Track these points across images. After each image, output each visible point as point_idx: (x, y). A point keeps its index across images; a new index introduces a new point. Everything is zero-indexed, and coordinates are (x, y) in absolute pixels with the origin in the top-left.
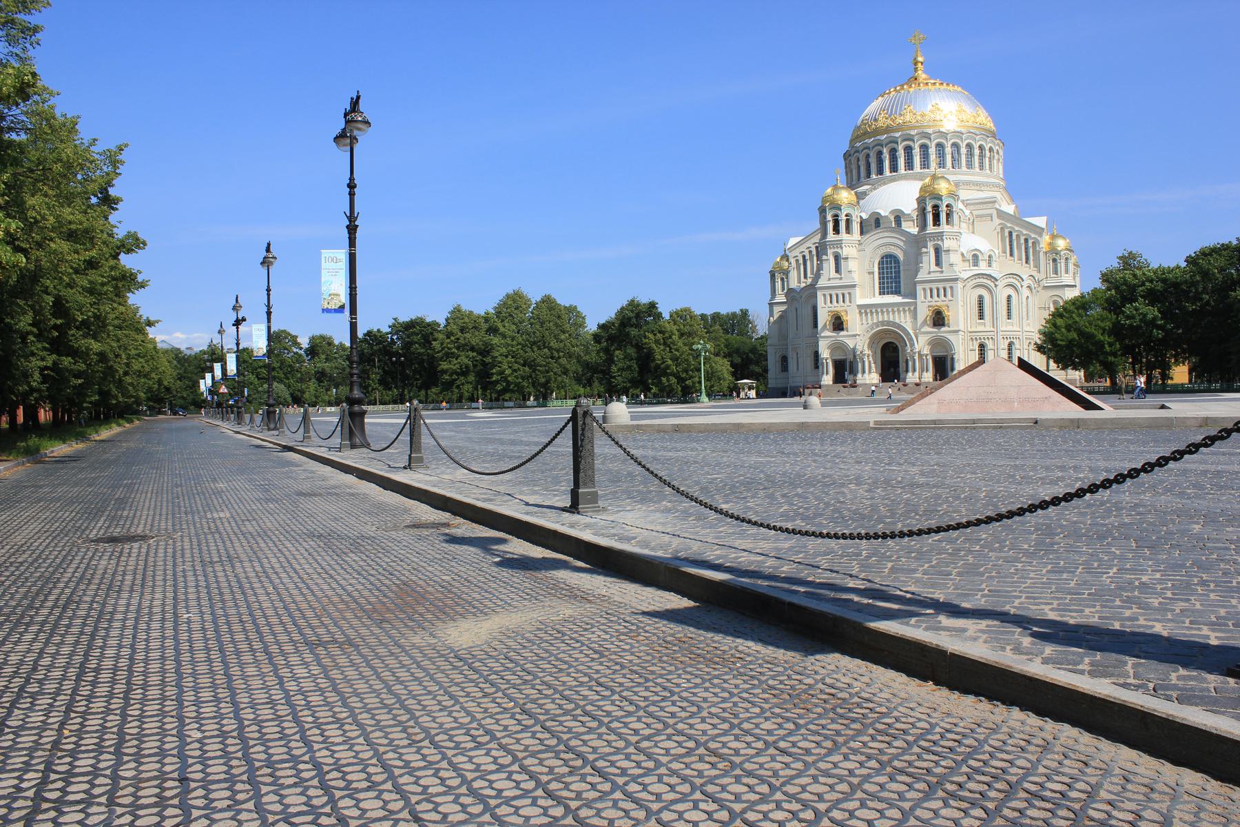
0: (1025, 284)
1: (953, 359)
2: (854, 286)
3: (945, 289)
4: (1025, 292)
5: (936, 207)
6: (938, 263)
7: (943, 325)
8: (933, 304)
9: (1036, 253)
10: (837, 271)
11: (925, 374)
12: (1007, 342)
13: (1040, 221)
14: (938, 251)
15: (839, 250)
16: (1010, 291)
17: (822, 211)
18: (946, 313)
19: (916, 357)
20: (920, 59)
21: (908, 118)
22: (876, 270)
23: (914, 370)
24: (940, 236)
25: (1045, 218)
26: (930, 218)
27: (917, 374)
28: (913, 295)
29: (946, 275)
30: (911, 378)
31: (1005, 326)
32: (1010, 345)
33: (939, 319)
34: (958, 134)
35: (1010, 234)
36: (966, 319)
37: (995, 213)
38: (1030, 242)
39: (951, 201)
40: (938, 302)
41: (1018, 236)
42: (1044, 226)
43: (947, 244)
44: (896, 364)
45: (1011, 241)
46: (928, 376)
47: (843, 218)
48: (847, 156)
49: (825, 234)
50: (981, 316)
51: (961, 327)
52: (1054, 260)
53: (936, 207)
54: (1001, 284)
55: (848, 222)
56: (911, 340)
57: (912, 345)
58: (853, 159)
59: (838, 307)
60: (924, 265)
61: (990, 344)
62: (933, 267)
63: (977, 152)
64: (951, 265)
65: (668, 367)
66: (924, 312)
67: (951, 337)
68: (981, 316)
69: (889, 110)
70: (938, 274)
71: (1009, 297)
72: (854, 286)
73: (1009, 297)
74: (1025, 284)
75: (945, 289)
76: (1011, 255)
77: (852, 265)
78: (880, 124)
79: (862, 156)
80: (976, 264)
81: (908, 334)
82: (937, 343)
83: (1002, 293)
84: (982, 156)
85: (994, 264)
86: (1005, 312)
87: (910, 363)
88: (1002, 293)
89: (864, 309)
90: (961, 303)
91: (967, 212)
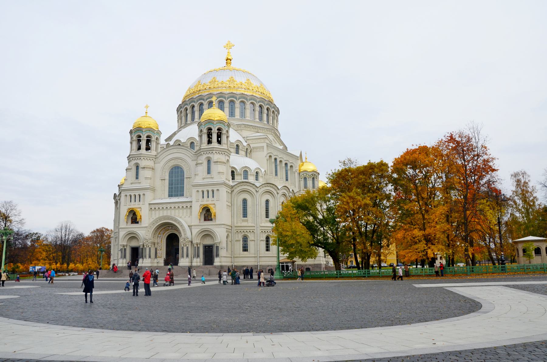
1: (217, 247)
3: (213, 191)
5: (210, 129)
7: (211, 220)
11: (195, 260)
15: (138, 161)
17: (131, 132)
18: (213, 211)
22: (167, 177)
30: (184, 262)
32: (268, 238)
33: (207, 214)
37: (265, 145)
38: (289, 165)
43: (215, 157)
46: (198, 262)
48: (178, 111)
50: (245, 215)
52: (305, 179)
55: (148, 141)
59: (134, 205)
61: (251, 237)
66: (197, 209)
71: (267, 202)
73: (267, 202)
74: (281, 192)
75: (213, 191)
76: (276, 175)
79: (183, 110)
80: (246, 177)
81: (182, 226)
84: (261, 112)
85: (260, 179)
89: (153, 207)
91: (245, 144)
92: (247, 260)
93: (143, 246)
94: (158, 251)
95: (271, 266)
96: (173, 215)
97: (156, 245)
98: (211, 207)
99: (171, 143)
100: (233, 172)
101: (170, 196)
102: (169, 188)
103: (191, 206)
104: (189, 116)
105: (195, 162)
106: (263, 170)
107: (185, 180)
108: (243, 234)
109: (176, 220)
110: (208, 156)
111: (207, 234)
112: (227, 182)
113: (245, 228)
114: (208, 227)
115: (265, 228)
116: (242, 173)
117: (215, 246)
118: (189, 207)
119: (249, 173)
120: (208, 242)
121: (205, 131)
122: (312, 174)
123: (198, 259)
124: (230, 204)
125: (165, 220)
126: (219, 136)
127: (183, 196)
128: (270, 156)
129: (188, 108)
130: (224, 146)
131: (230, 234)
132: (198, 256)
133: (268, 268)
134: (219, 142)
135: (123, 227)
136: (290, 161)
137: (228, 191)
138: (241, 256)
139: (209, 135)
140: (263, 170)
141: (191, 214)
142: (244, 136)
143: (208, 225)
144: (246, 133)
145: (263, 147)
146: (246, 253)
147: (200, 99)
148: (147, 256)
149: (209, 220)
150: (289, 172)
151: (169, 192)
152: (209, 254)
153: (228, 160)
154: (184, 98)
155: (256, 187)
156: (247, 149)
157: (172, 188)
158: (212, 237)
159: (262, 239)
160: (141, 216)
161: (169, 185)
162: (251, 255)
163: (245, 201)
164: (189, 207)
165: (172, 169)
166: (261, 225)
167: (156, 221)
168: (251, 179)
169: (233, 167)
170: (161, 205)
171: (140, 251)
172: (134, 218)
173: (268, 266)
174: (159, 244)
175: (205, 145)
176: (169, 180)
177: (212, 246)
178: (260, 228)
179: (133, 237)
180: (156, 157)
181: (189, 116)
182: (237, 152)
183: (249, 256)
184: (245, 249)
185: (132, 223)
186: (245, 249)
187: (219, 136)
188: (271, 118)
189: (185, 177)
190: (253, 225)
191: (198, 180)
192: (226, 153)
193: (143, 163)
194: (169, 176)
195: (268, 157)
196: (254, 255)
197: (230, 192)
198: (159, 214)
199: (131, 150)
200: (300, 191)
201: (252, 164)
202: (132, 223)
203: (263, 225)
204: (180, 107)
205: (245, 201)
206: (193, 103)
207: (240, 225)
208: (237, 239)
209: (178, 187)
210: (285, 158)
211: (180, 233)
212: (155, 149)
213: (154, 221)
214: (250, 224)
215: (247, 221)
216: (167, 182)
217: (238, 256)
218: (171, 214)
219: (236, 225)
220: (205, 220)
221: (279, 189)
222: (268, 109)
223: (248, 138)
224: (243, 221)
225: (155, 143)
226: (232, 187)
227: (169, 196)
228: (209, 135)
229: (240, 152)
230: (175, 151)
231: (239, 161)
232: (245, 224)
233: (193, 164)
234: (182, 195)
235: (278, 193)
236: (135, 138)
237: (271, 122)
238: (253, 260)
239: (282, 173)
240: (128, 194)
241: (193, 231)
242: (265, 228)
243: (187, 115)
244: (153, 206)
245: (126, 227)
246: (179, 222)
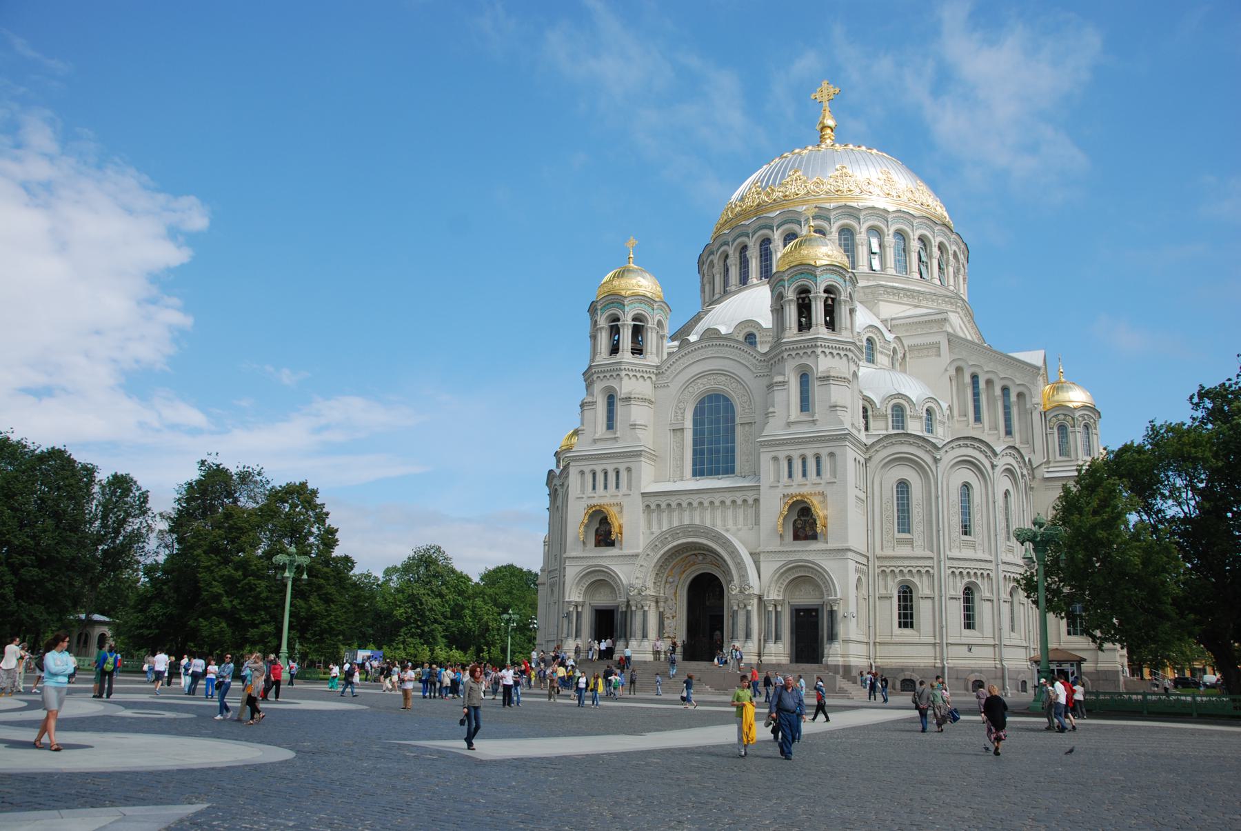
0: (1002, 462)
1: (832, 613)
2: (638, 454)
3: (818, 459)
4: (1004, 483)
5: (804, 292)
6: (805, 403)
7: (814, 537)
8: (793, 490)
9: (1026, 413)
10: (610, 425)
11: (771, 647)
12: (961, 585)
13: (1034, 357)
14: (805, 378)
16: (967, 475)
17: (593, 309)
18: (819, 511)
19: (753, 606)
20: (830, 122)
21: (792, 189)
22: (689, 424)
23: (748, 636)
24: (811, 348)
25: (1041, 353)
26: (792, 313)
27: (752, 646)
28: (756, 474)
29: (825, 426)
31: (955, 548)
32: (969, 592)
33: (803, 522)
34: (883, 214)
35: (975, 378)
36: (870, 530)
39: (836, 280)
40: (802, 487)
41: (989, 382)
42: (1040, 363)
44: (717, 622)
45: (976, 395)
46: (779, 652)
47: (627, 322)
48: (701, 263)
49: (594, 353)
50: (904, 524)
51: (852, 543)
52: (1062, 429)
53: (804, 292)
54: (948, 457)
55: (637, 331)
56: (740, 565)
57: (744, 576)
58: (705, 267)
59: (604, 498)
60: (779, 409)
61: (922, 587)
62: (795, 413)
63: (915, 245)
64: (834, 407)
65: (216, 598)
66: (773, 508)
67: (829, 565)
68: (904, 524)
69: (765, 186)
70: (804, 428)
72: (638, 454)
73: (966, 486)
74: (1002, 462)
75: (818, 459)
76: (978, 419)
77: (639, 413)
78: (748, 202)
79: (715, 258)
81: (734, 553)
82: (803, 575)
83: (952, 479)
86: (956, 521)
87: (741, 620)
88: (952, 479)
89: (655, 503)
90: (852, 492)
92: (911, 652)
93: (628, 605)
94: (667, 622)
95: (981, 672)
96: (708, 524)
97: (661, 604)
98: (816, 503)
99: (693, 338)
100: (865, 410)
101: (698, 472)
102: (695, 452)
103: (757, 501)
104: (734, 273)
105: (765, 381)
106: (945, 406)
107: (738, 430)
108: (900, 578)
109: (718, 537)
110: (803, 361)
111: (803, 575)
112: (855, 432)
113: (906, 563)
114: (804, 557)
115: (962, 564)
116: (889, 411)
117: (826, 610)
118: (750, 501)
119: (908, 412)
120: (805, 599)
121: (791, 295)
122: (1082, 416)
123: (780, 645)
124: (863, 496)
125: (685, 536)
126: (830, 311)
127: (733, 472)
128: (959, 370)
129: (731, 252)
130: (845, 336)
131: (864, 579)
132: (778, 638)
133: (973, 677)
134: (831, 324)
135: (574, 554)
136: (1018, 380)
137: (858, 458)
138: (896, 639)
139: (804, 308)
140: (945, 406)
141: (757, 523)
142: (882, 317)
143: (808, 552)
144: (890, 309)
145: (937, 347)
146: (907, 631)
147: (761, 228)
148: (639, 633)
149: (806, 538)
150: (1015, 411)
151: (694, 464)
152: (810, 631)
153: (855, 374)
154: (718, 229)
155: (934, 446)
156: (895, 351)
157: (702, 453)
158: (817, 586)
159: (952, 593)
160: (621, 527)
161: (695, 444)
162: (924, 640)
163: (903, 486)
164: (750, 501)
165: (702, 402)
166: (951, 555)
167: (663, 539)
168: (915, 427)
169: (866, 399)
170: (673, 498)
171: (618, 619)
172: (603, 531)
173: (973, 671)
174: (670, 602)
175: (792, 333)
176: (695, 433)
177: (816, 610)
178: (949, 564)
179: (600, 581)
180: (659, 371)
181: (734, 273)
182: (871, 360)
183: (916, 640)
184: (906, 620)
185: (598, 543)
186: (906, 620)
187: (830, 311)
188: (951, 270)
189: (738, 420)
190: (928, 553)
191: (775, 429)
192: (850, 355)
193: (626, 386)
194: (695, 423)
195: (952, 372)
196: (931, 640)
197: (862, 461)
198: (670, 522)
199: (594, 353)
200: (1048, 462)
201: (914, 390)
202: (598, 543)
203: (955, 553)
204: (709, 250)
205: (903, 486)
206: (744, 239)
207: (888, 552)
208: (883, 591)
209: (718, 451)
210: (1002, 374)
211: (728, 572)
212: (654, 350)
213: (657, 538)
214: (919, 552)
215: (910, 542)
216: (689, 436)
217: (888, 640)
218: (702, 519)
219: (879, 552)
220: (796, 537)
221: (995, 454)
222: (941, 247)
223: (894, 322)
224: (900, 541)
225: (654, 335)
226: (867, 448)
227: (695, 474)
228: (804, 308)
229: (879, 358)
230: (709, 352)
231: (879, 381)
232: (904, 551)
233: (757, 386)
234: (729, 470)
235: (993, 466)
236: (603, 322)
237: (952, 282)
238: (929, 651)
239: (993, 413)
240: (587, 469)
241: (762, 565)
242: (962, 564)
243: (727, 270)
244: (652, 499)
245: (581, 554)
246: (727, 544)
